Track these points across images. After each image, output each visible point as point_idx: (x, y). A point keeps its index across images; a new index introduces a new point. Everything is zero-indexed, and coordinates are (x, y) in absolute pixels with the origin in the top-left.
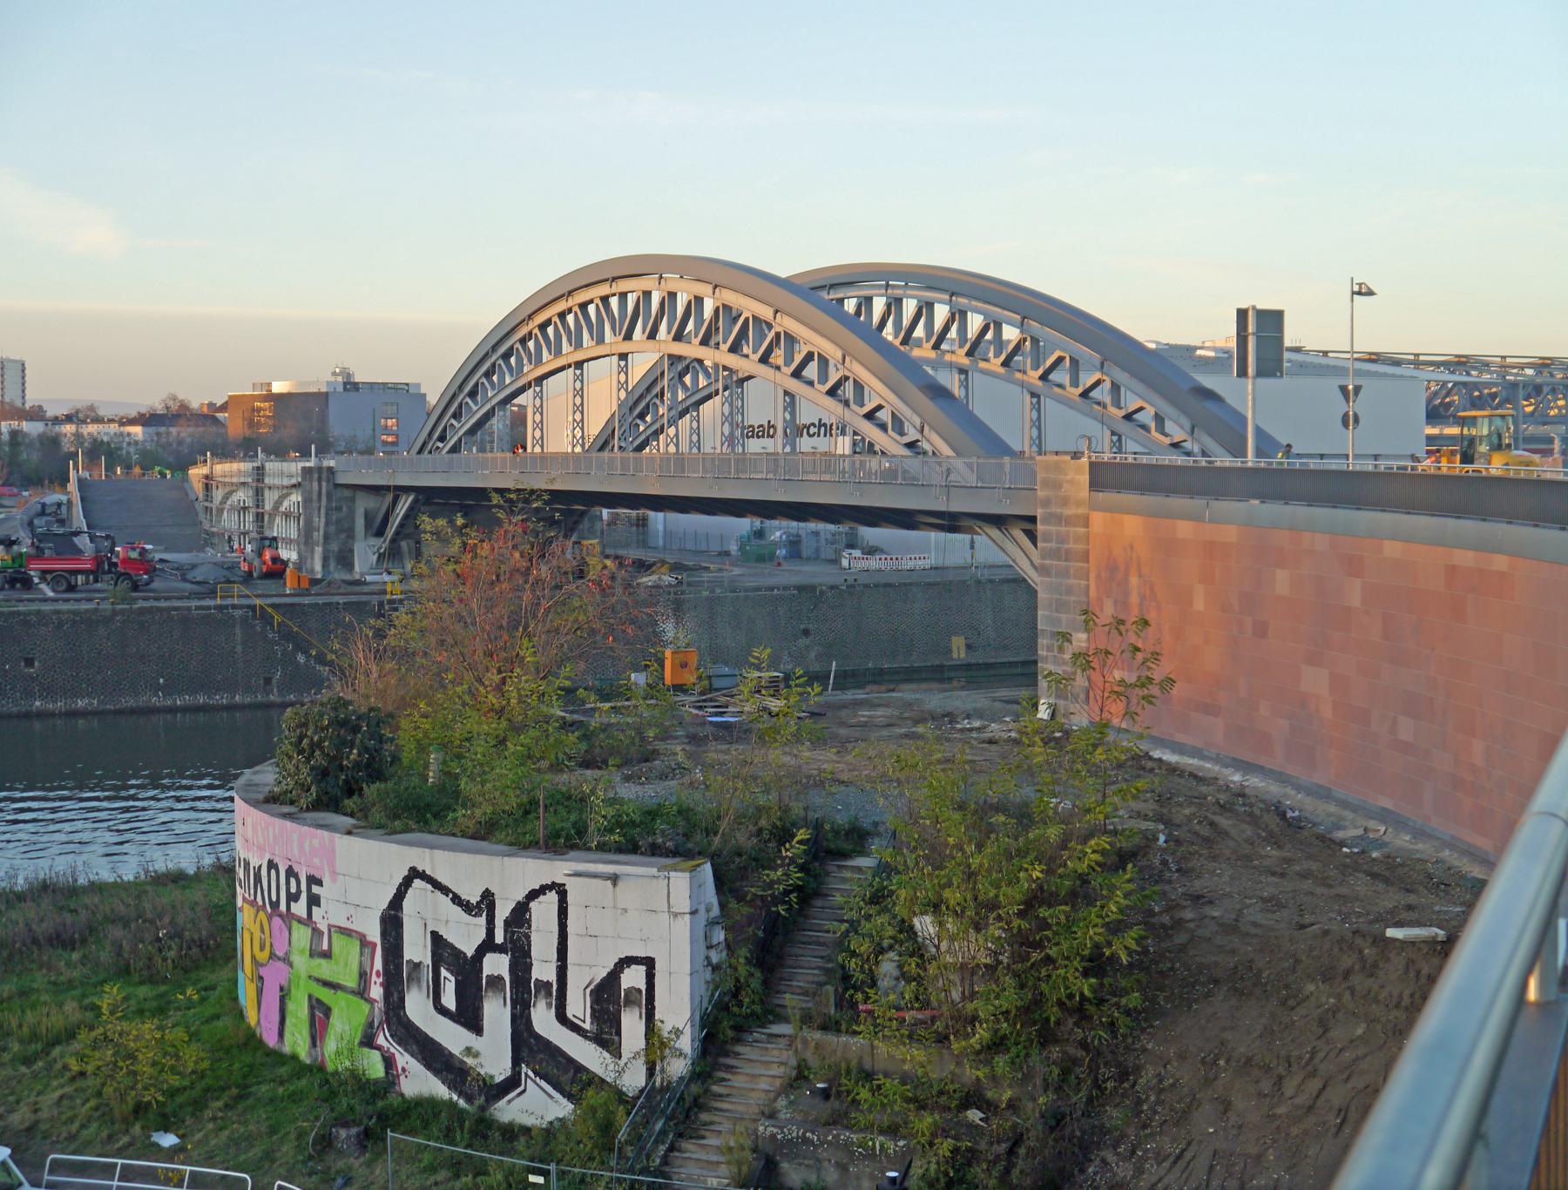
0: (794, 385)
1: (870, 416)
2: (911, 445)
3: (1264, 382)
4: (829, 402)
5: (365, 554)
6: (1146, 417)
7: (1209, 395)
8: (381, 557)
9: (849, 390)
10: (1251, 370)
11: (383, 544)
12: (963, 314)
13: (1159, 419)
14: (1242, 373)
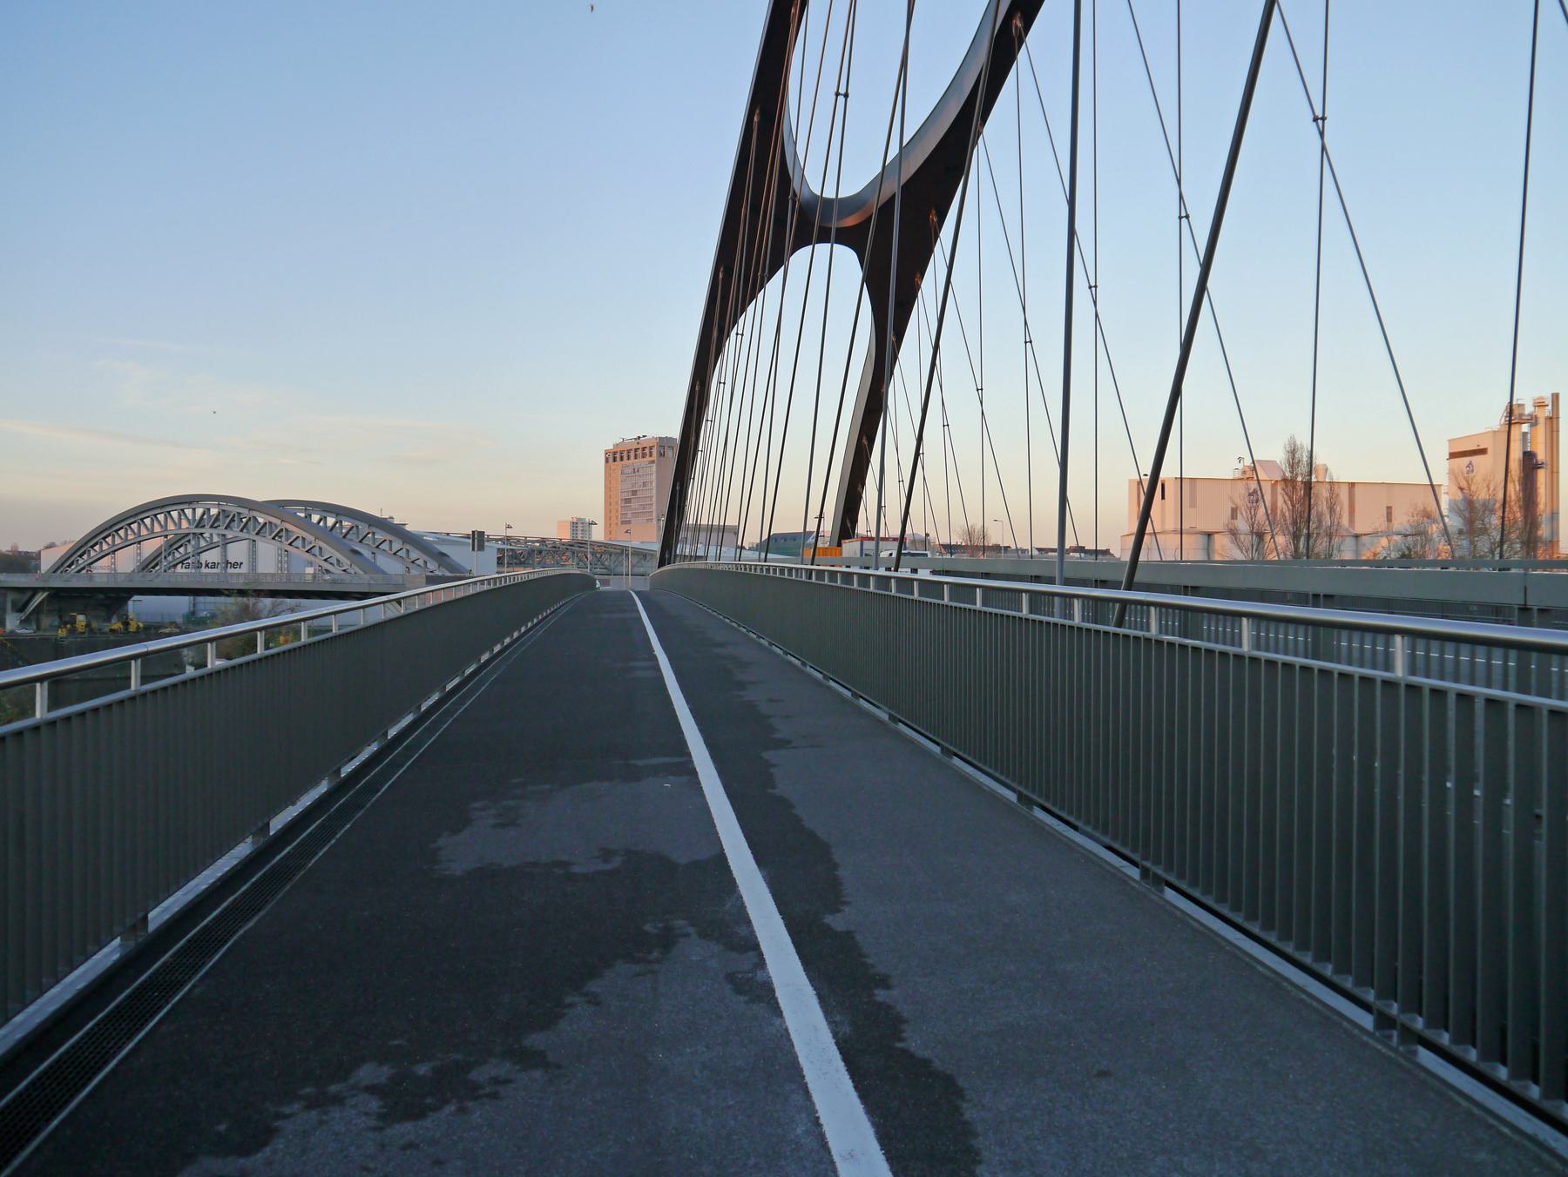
0: (289, 548)
1: (325, 560)
2: (344, 571)
3: (479, 552)
4: (307, 555)
6: (420, 562)
7: (444, 555)
8: (22, 622)
9: (316, 551)
10: (476, 549)
11: (23, 616)
12: (325, 518)
13: (425, 562)
14: (473, 549)
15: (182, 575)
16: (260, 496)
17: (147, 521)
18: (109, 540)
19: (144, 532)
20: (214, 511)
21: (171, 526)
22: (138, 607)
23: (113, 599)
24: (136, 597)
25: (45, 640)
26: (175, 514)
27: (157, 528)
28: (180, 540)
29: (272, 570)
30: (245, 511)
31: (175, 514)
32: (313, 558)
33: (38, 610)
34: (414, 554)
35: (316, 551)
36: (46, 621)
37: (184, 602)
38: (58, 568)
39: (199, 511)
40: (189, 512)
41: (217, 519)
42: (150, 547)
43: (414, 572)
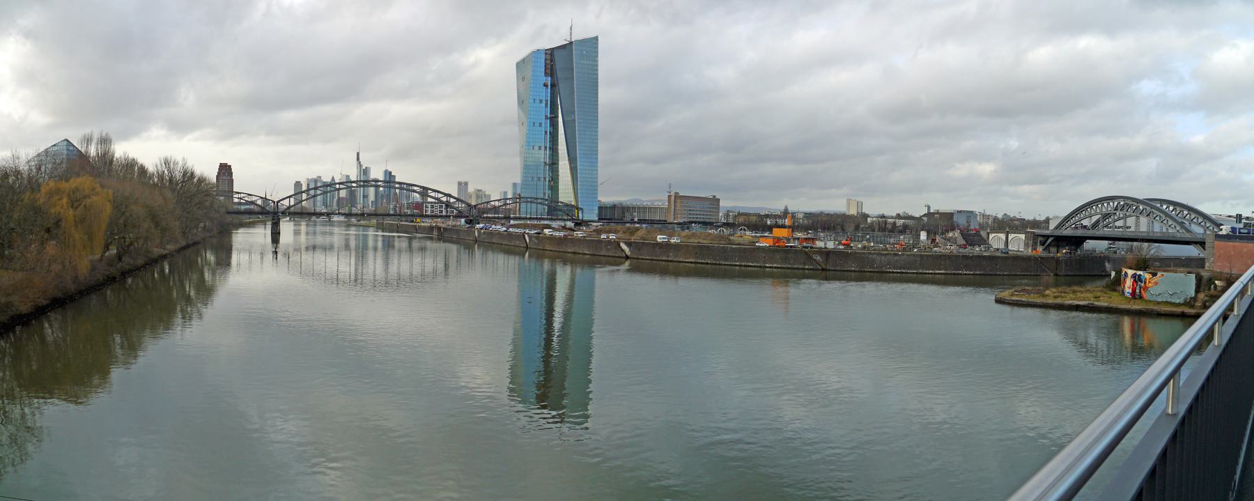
5: (1040, 249)
6: (1211, 228)
13: (1213, 228)
15: (1107, 231)
16: (1141, 197)
17: (1094, 207)
18: (1079, 215)
19: (1093, 212)
20: (1122, 203)
21: (1104, 210)
22: (1089, 245)
23: (1077, 241)
24: (1087, 241)
25: (1053, 258)
26: (1105, 204)
27: (1098, 211)
28: (1106, 216)
29: (1145, 230)
30: (1135, 203)
31: (1105, 204)
32: (1163, 225)
33: (1049, 245)
34: (1208, 225)
35: (1165, 222)
36: (1053, 249)
37: (1106, 243)
38: (1058, 227)
39: (1116, 203)
40: (1111, 204)
41: (1123, 206)
42: (1095, 219)
43: (1208, 232)
